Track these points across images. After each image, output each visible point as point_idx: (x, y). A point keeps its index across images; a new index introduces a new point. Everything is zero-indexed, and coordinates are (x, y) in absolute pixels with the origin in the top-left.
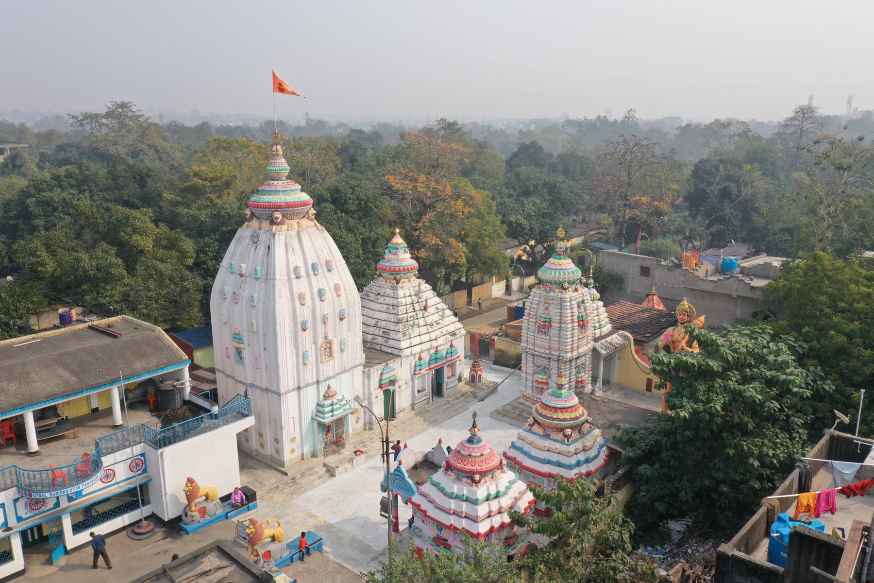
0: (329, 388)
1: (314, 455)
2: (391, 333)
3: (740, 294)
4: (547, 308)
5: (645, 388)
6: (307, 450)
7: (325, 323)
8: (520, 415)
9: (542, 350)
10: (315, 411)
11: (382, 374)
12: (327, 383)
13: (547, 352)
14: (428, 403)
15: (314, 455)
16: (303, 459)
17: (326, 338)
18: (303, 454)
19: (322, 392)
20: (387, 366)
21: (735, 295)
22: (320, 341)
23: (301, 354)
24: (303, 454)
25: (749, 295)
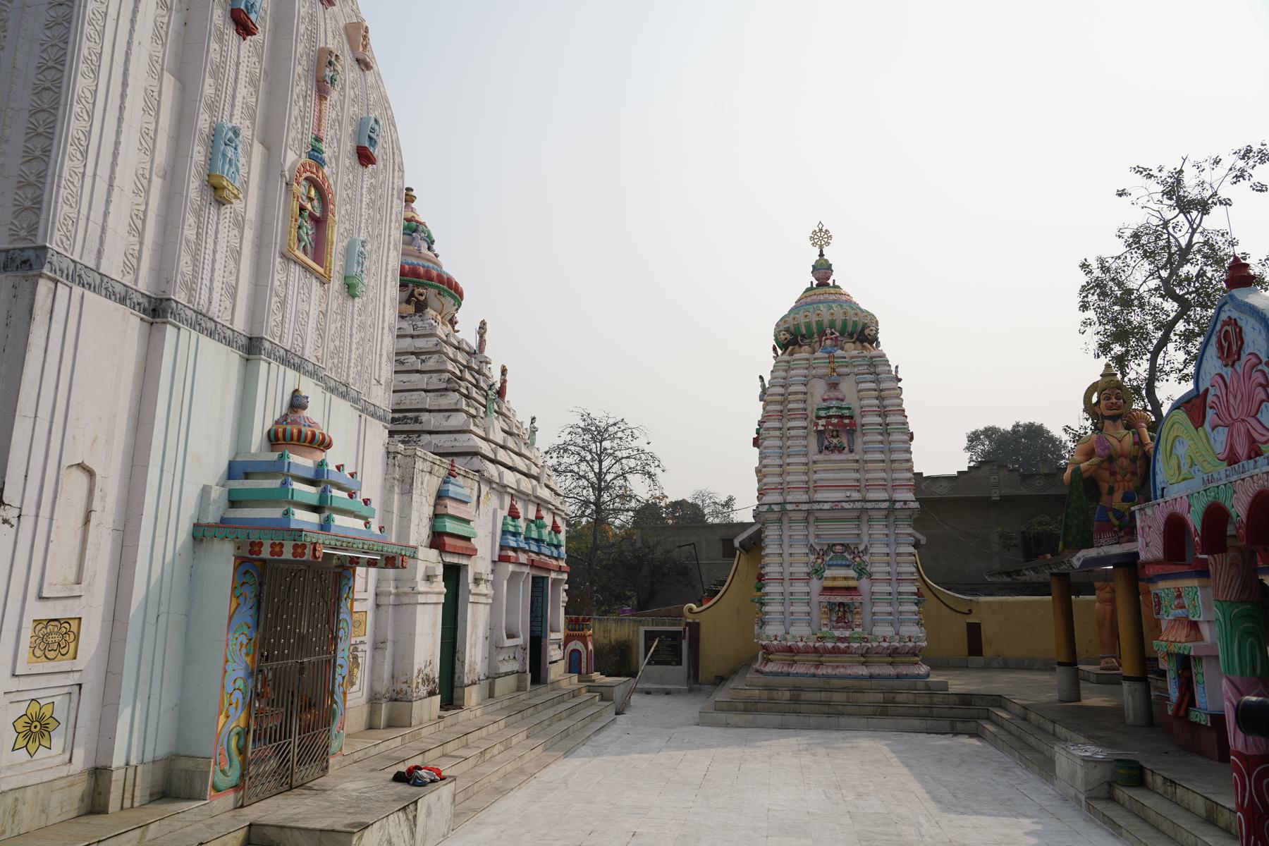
0: (297, 403)
1: (174, 784)
2: (425, 417)
3: (1005, 492)
4: (834, 386)
5: (963, 647)
6: (132, 745)
7: (322, 94)
8: (795, 700)
9: (839, 495)
10: (218, 494)
11: (441, 496)
12: (291, 379)
13: (856, 495)
14: (520, 688)
15: (174, 784)
16: (95, 804)
17: (315, 154)
18: (99, 774)
19: (265, 416)
20: (451, 474)
21: (995, 497)
22: (292, 158)
23: (204, 122)
24: (99, 774)
25: (1023, 491)
